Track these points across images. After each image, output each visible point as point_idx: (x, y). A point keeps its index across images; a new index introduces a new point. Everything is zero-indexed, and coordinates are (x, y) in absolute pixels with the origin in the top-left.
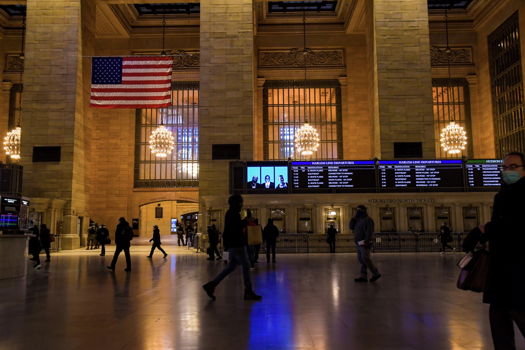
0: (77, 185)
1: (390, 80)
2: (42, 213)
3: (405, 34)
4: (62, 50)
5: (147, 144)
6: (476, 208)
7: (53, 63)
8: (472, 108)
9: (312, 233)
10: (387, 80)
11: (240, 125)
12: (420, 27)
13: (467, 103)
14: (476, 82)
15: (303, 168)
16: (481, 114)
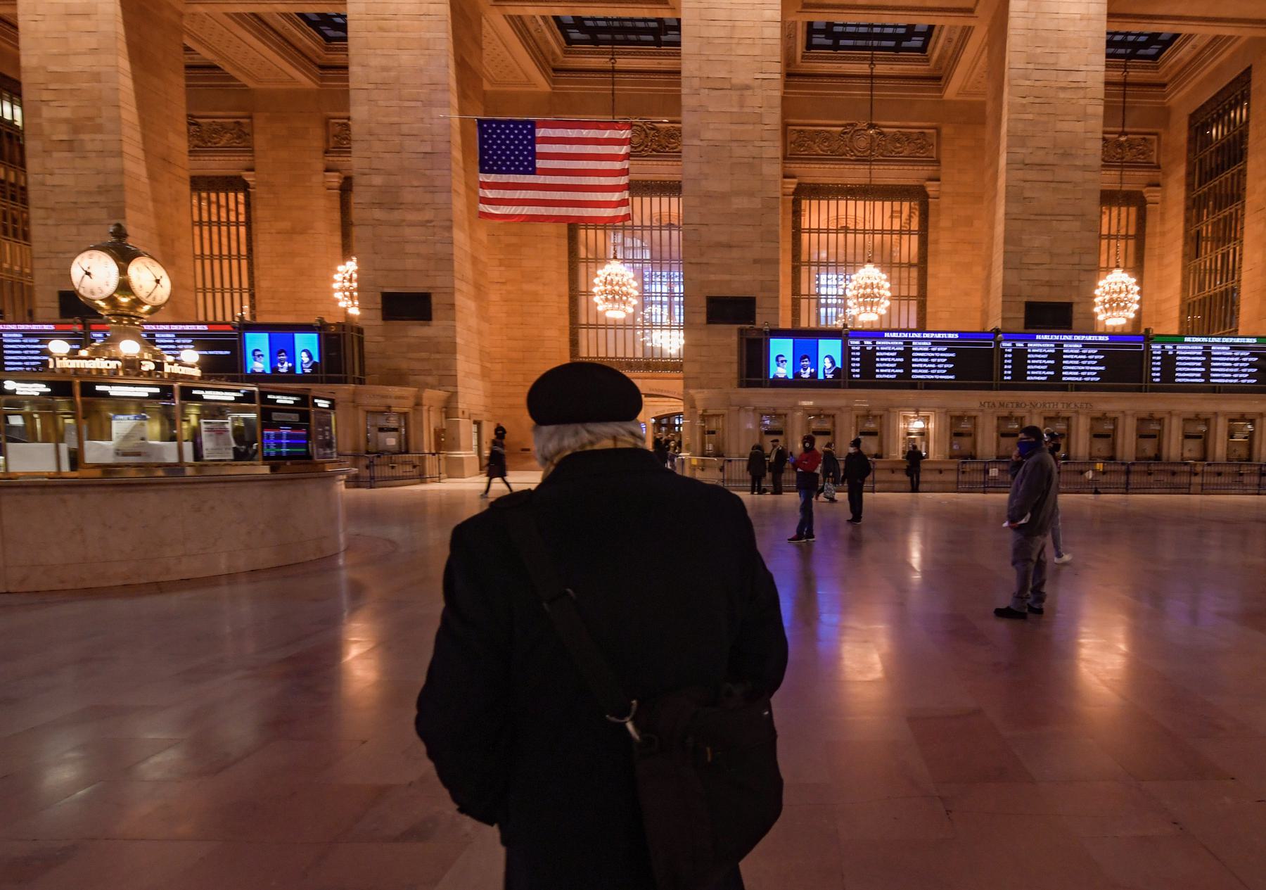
0: (466, 366)
1: (1028, 185)
2: (405, 414)
3: (1062, 95)
4: (419, 104)
5: (589, 294)
6: (1160, 421)
7: (405, 129)
8: (1147, 246)
9: (881, 457)
10: (1023, 184)
11: (756, 261)
12: (1089, 84)
13: (1140, 238)
14: (1158, 199)
15: (867, 342)
16: (1161, 257)
